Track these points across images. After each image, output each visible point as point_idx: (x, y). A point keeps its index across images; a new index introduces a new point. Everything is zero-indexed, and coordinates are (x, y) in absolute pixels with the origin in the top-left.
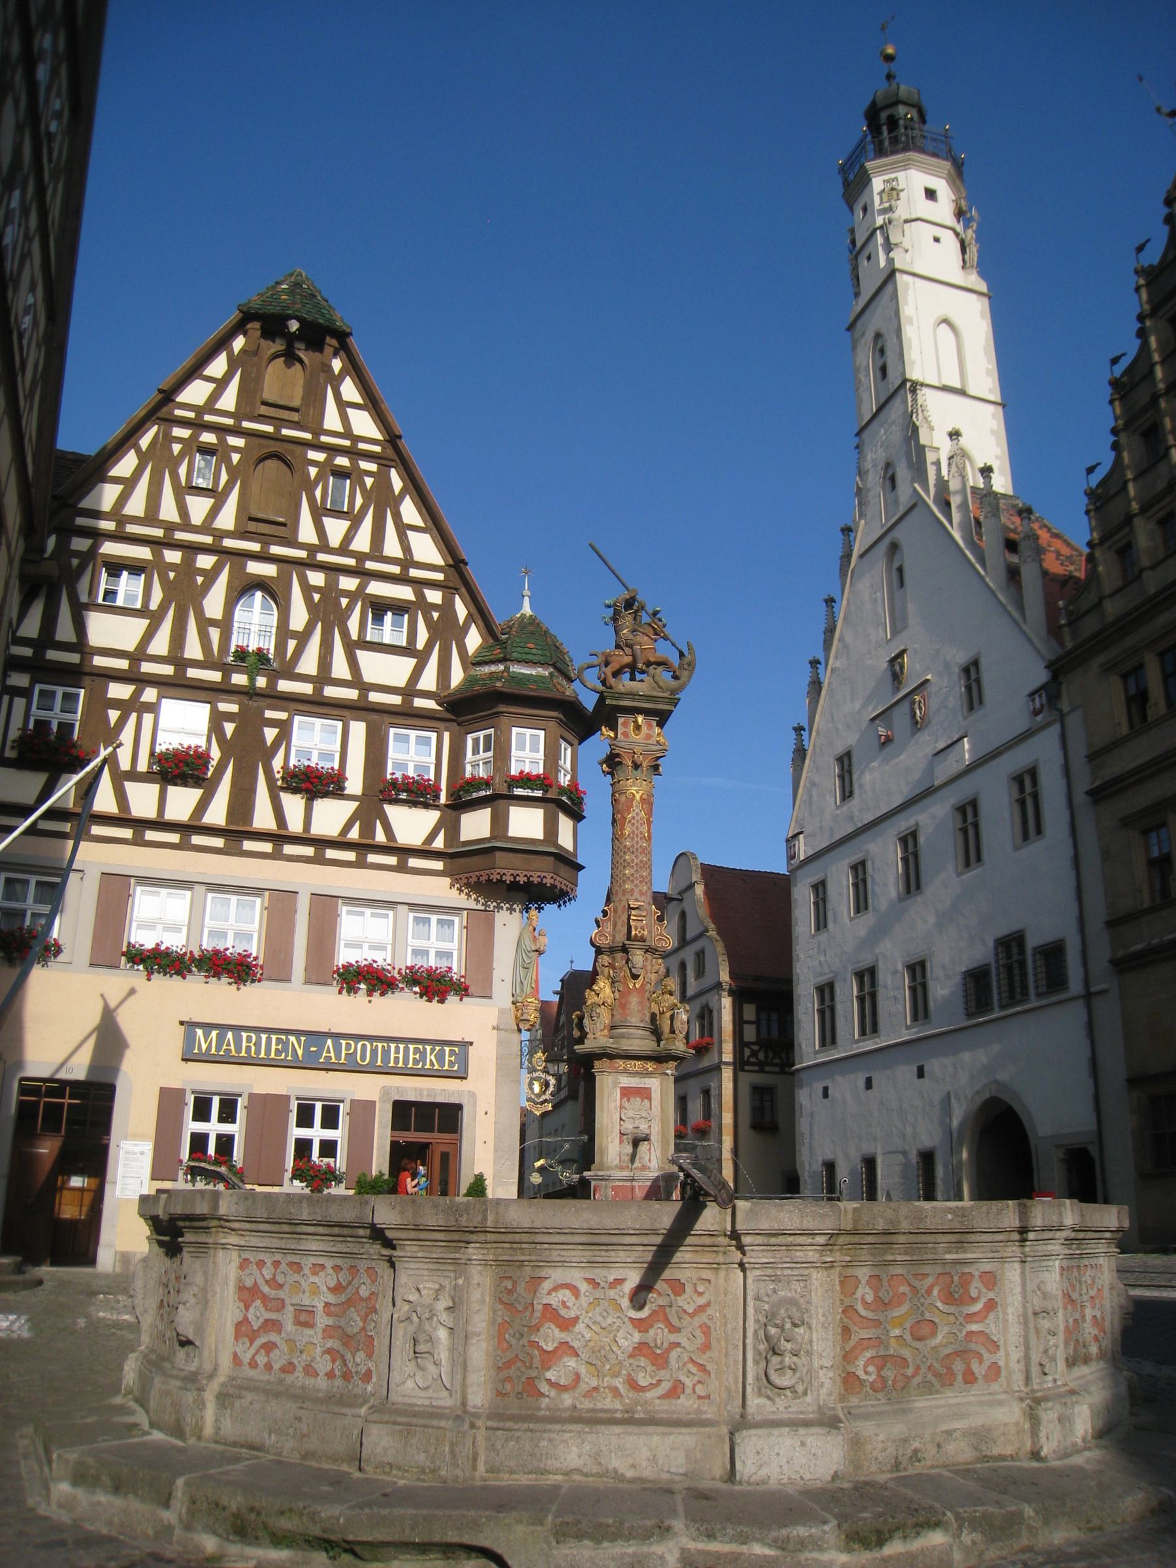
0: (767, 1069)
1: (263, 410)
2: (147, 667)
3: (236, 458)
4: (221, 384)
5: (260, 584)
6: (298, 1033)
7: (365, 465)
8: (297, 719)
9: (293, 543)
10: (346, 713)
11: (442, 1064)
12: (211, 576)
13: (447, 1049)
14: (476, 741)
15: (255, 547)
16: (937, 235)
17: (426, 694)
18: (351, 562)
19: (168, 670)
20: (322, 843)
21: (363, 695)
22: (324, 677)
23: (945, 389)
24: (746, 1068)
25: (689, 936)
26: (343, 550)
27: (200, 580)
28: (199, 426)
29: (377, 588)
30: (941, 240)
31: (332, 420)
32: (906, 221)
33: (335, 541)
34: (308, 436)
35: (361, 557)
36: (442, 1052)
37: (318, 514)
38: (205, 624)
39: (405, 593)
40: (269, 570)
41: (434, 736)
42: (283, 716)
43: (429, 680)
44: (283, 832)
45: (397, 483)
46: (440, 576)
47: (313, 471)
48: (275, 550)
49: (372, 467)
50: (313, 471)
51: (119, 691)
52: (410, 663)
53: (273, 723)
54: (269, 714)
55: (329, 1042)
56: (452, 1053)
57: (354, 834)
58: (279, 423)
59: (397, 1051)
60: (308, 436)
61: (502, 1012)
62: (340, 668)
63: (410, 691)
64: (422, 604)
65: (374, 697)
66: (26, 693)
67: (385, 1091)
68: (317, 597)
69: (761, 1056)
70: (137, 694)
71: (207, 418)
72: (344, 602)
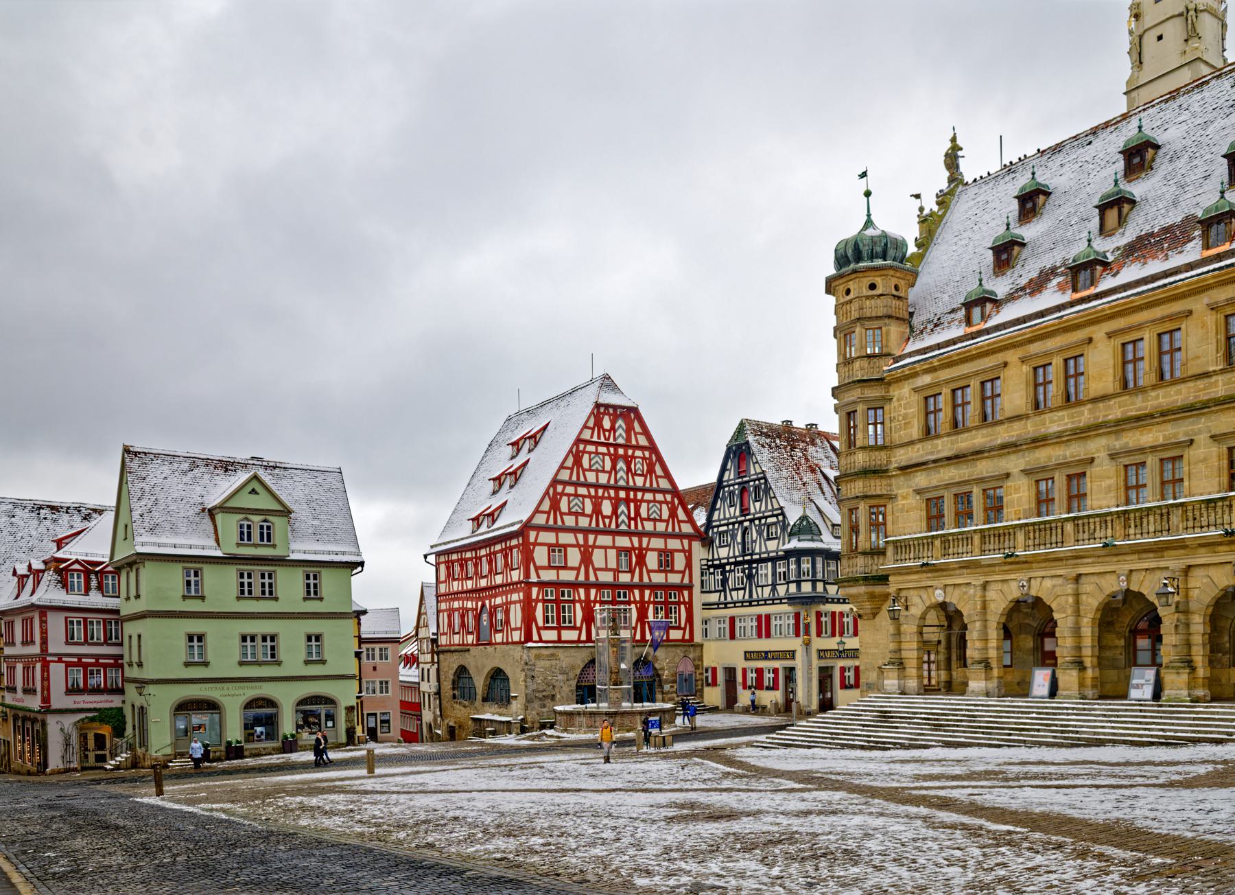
4: (730, 470)
5: (746, 528)
20: (765, 600)
26: (760, 512)
28: (729, 486)
29: (770, 520)
31: (752, 472)
35: (764, 512)
38: (738, 544)
39: (774, 519)
42: (754, 565)
46: (779, 511)
48: (748, 517)
51: (728, 568)
52: (777, 541)
62: (763, 549)
65: (771, 555)
66: (713, 573)
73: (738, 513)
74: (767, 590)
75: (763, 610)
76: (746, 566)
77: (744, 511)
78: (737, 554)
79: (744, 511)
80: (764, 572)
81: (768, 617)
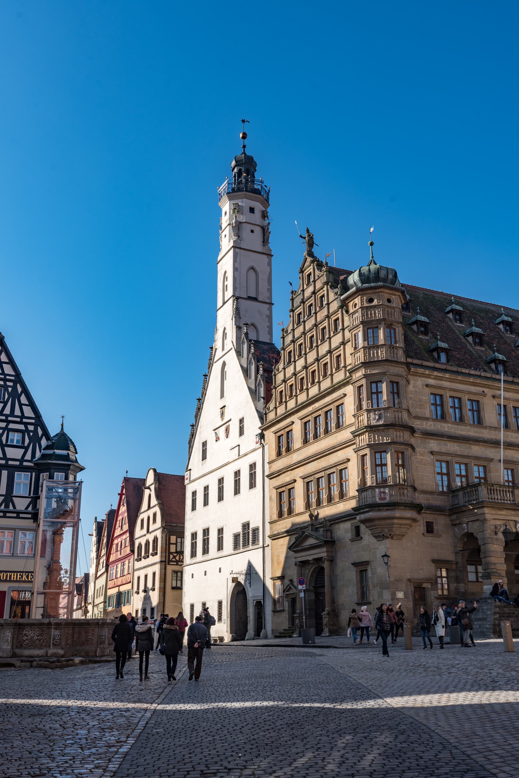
0: (179, 563)
7: (8, 384)
11: (28, 578)
14: (43, 476)
16: (252, 229)
17: (27, 461)
23: (250, 298)
24: (171, 563)
25: (152, 505)
29: (11, 426)
30: (254, 232)
32: (240, 223)
35: (7, 416)
39: (22, 427)
41: (29, 474)
43: (28, 456)
45: (20, 390)
46: (33, 421)
49: (11, 384)
52: (22, 451)
59: (14, 575)
63: (22, 460)
64: (27, 431)
65: (10, 463)
69: (177, 558)
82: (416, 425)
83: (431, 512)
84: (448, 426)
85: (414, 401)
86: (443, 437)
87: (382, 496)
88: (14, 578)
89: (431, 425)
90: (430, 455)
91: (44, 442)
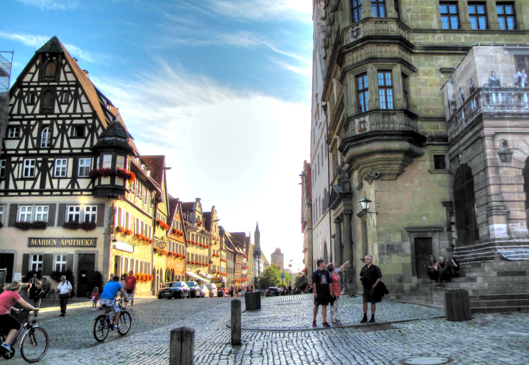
1: (46, 79)
2: (20, 152)
3: (39, 93)
4: (34, 74)
5: (46, 125)
6: (55, 239)
8: (57, 160)
9: (53, 113)
10: (68, 156)
11: (89, 244)
12: (34, 126)
13: (91, 240)
15: (44, 116)
17: (87, 148)
18: (68, 116)
19: (24, 152)
20: (62, 191)
21: (71, 151)
22: (62, 148)
26: (66, 113)
27: (31, 127)
28: (29, 87)
31: (62, 78)
33: (64, 111)
34: (56, 84)
35: (70, 114)
36: (90, 241)
37: (60, 104)
38: (33, 139)
40: (48, 122)
42: (52, 159)
43: (88, 145)
44: (52, 189)
46: (91, 116)
47: (58, 93)
48: (49, 116)
49: (73, 88)
50: (58, 93)
51: (14, 159)
53: (50, 162)
54: (50, 159)
55: (63, 240)
56: (92, 241)
57: (70, 187)
58: (48, 82)
59: (79, 241)
60: (56, 84)
61: (106, 229)
62: (66, 145)
63: (83, 148)
65: (74, 151)
67: (76, 251)
68: (60, 127)
70: (18, 159)
71: (31, 84)
72: (67, 127)
73: (37, 111)
74: (64, 184)
75: (57, 200)
76: (40, 159)
77: (46, 110)
78: (30, 146)
79: (46, 110)
80: (61, 166)
81: (63, 207)
82: (417, 40)
83: (440, 143)
84: (465, 37)
85: (414, 12)
86: (458, 50)
87: (362, 126)
88: (78, 243)
89: (439, 38)
90: (439, 73)
91: (100, 132)
